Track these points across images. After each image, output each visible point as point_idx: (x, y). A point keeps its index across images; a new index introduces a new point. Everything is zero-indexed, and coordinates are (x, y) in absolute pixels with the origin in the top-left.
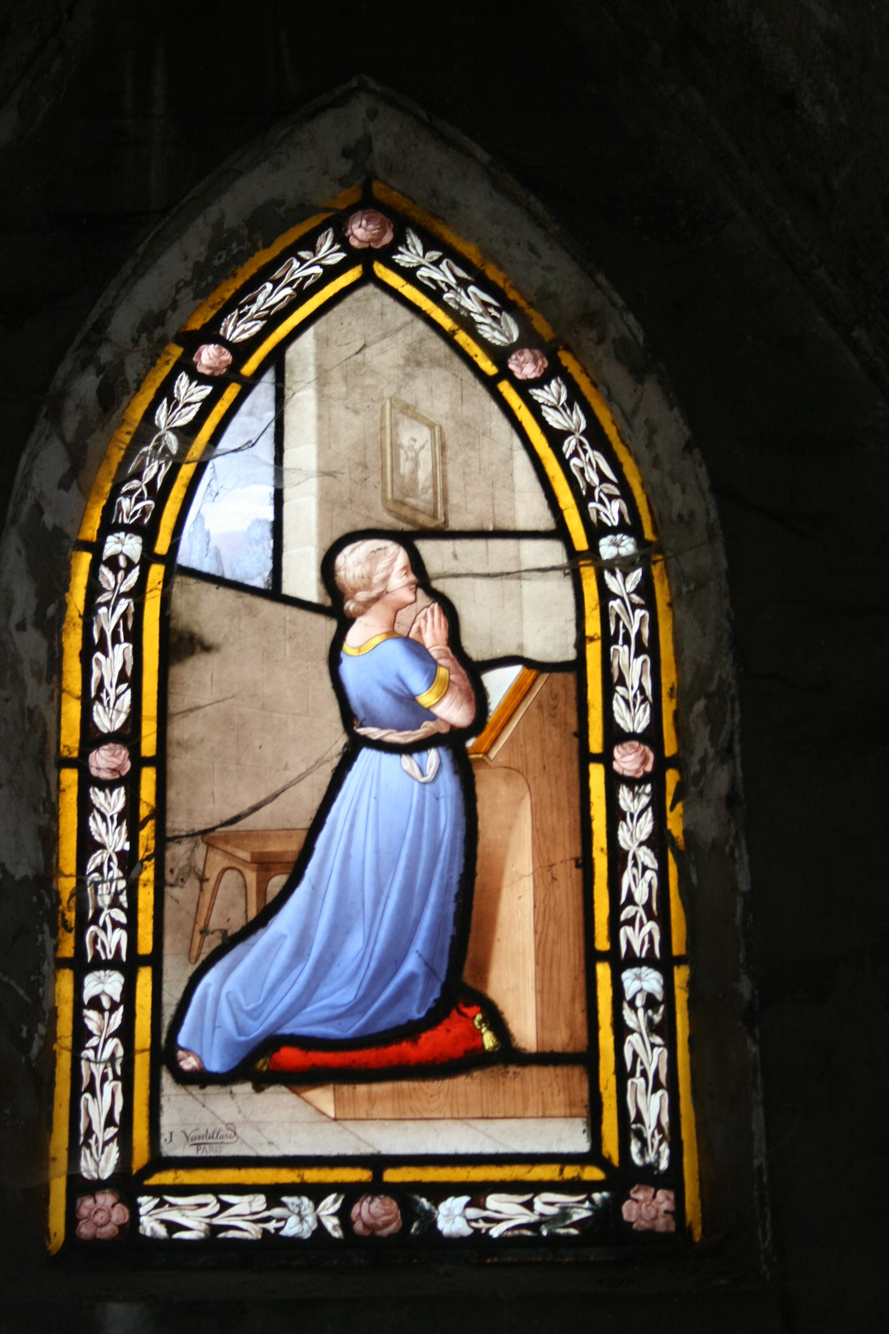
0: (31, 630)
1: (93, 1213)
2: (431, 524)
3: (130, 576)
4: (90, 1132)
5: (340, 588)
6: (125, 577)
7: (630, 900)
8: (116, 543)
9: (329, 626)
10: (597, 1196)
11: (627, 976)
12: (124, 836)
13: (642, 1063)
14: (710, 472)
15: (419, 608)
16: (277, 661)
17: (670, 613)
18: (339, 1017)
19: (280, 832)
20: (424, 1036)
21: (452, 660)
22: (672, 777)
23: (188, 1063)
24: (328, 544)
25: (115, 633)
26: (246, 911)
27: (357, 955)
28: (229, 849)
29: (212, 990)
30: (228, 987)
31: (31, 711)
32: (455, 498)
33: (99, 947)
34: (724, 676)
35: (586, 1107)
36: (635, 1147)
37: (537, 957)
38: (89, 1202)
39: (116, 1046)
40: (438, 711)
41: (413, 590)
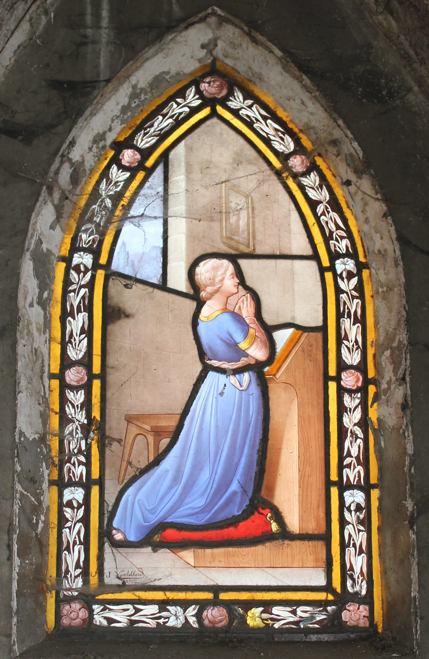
0: (35, 305)
1: (69, 613)
2: (246, 250)
3: (86, 276)
4: (67, 571)
5: (198, 284)
6: (84, 277)
7: (349, 455)
8: (79, 258)
9: (193, 305)
10: (329, 608)
11: (347, 494)
12: (84, 416)
13: (353, 540)
14: (396, 230)
15: (240, 297)
16: (164, 323)
17: (372, 301)
18: (197, 513)
19: (166, 415)
20: (241, 524)
21: (257, 325)
22: (372, 389)
23: (118, 537)
24: (191, 261)
25: (79, 307)
26: (148, 457)
27: (206, 481)
28: (139, 424)
29: (130, 499)
30: (138, 497)
31: (36, 350)
32: (259, 237)
33: (71, 475)
34: (401, 339)
35: (324, 562)
36: (349, 583)
37: (300, 481)
38: (67, 607)
39: (81, 526)
40: (249, 352)
41: (237, 286)
